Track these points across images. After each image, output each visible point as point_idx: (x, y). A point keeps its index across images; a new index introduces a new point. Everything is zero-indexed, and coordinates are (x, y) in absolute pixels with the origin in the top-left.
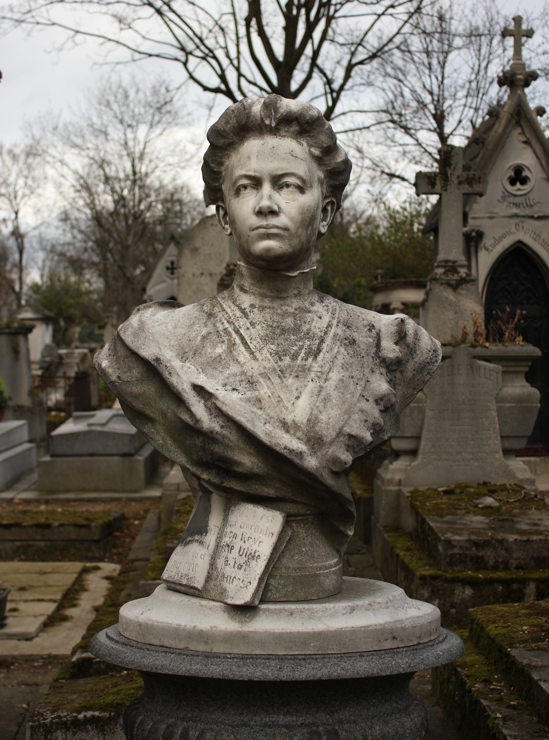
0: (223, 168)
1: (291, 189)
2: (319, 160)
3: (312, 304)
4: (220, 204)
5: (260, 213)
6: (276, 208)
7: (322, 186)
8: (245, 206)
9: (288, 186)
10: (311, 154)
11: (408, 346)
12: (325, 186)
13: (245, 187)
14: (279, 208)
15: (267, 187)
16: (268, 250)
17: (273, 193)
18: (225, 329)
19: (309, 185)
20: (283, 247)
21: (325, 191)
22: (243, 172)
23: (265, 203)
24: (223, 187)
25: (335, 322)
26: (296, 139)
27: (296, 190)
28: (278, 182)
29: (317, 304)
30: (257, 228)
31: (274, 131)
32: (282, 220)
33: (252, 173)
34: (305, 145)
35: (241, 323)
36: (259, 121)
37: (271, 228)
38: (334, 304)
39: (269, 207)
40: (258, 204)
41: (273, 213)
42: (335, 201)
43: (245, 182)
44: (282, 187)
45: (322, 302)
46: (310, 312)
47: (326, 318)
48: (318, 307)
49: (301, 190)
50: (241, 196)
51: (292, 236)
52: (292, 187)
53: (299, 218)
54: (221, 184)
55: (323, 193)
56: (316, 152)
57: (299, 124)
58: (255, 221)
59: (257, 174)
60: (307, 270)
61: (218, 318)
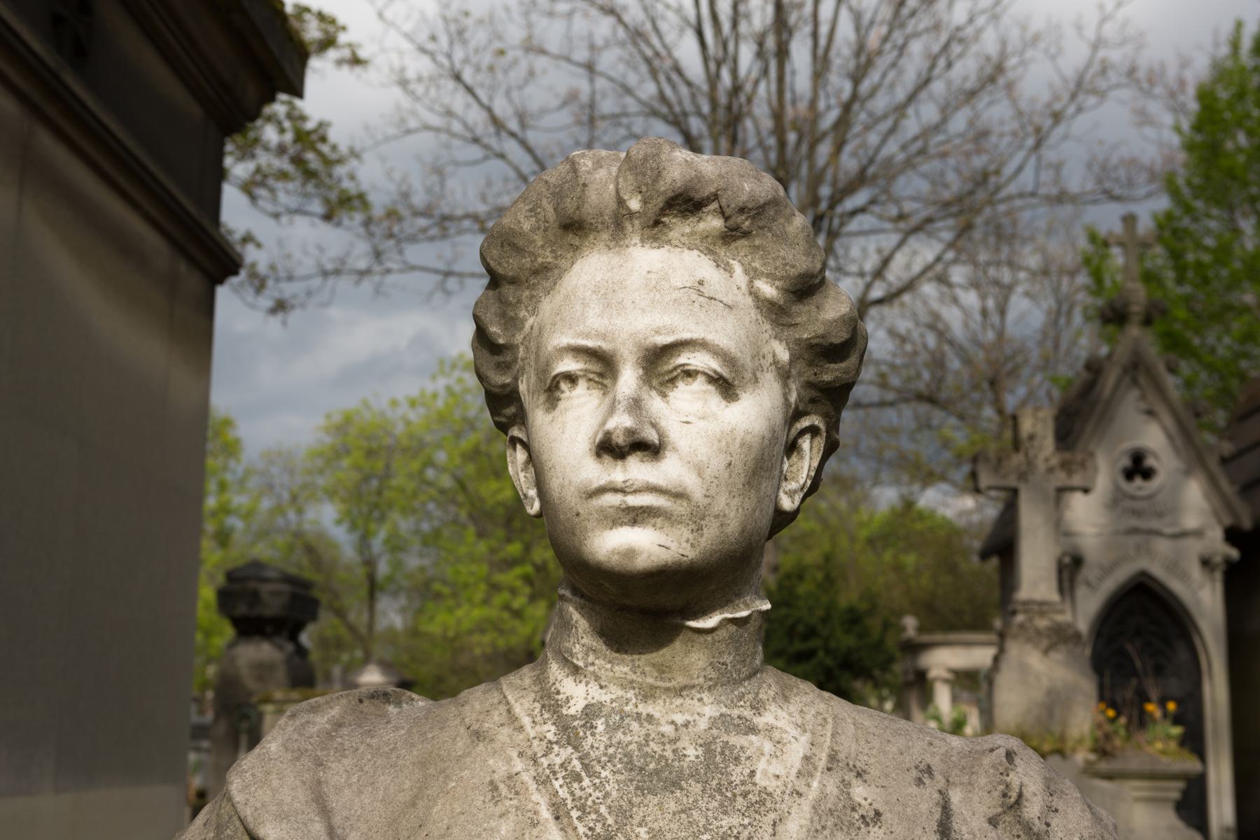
0: (519, 338)
1: (699, 384)
2: (776, 313)
3: (758, 707)
4: (516, 432)
5: (608, 449)
6: (651, 436)
7: (785, 385)
8: (569, 430)
9: (690, 374)
10: (754, 293)
11: (1027, 828)
12: (794, 387)
13: (571, 378)
14: (661, 435)
15: (629, 379)
16: (630, 553)
17: (645, 396)
18: (510, 777)
19: (748, 375)
20: (674, 546)
21: (793, 398)
22: (566, 340)
23: (621, 421)
24: (522, 387)
25: (822, 762)
26: (710, 252)
27: (711, 388)
28: (660, 363)
29: (773, 707)
30: (602, 490)
31: (655, 227)
32: (667, 471)
33: (590, 343)
34: (738, 269)
35: (558, 761)
36: (612, 205)
37: (635, 492)
38: (822, 707)
39: (630, 432)
40: (604, 423)
41: (650, 449)
42: (822, 426)
43: (569, 365)
44: (673, 381)
45: (786, 699)
46: (752, 730)
47: (797, 749)
48: (776, 716)
49: (726, 387)
50: (562, 405)
51: (697, 518)
52: (701, 379)
53: (717, 464)
54: (516, 379)
55: (787, 402)
56: (768, 290)
57: (722, 212)
58: (597, 472)
59: (605, 346)
60: (744, 614)
61: (497, 745)
